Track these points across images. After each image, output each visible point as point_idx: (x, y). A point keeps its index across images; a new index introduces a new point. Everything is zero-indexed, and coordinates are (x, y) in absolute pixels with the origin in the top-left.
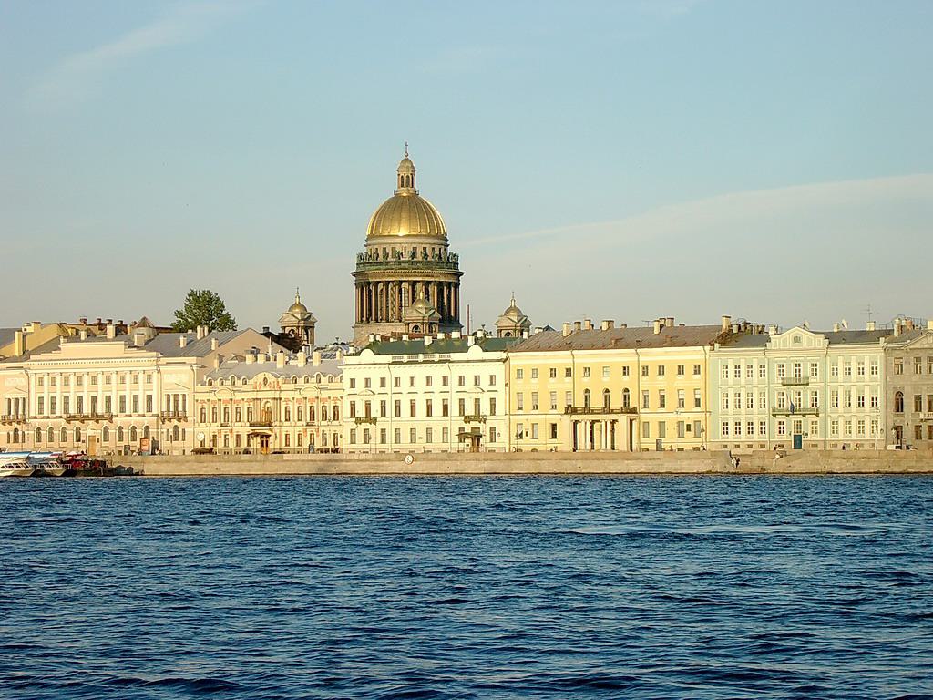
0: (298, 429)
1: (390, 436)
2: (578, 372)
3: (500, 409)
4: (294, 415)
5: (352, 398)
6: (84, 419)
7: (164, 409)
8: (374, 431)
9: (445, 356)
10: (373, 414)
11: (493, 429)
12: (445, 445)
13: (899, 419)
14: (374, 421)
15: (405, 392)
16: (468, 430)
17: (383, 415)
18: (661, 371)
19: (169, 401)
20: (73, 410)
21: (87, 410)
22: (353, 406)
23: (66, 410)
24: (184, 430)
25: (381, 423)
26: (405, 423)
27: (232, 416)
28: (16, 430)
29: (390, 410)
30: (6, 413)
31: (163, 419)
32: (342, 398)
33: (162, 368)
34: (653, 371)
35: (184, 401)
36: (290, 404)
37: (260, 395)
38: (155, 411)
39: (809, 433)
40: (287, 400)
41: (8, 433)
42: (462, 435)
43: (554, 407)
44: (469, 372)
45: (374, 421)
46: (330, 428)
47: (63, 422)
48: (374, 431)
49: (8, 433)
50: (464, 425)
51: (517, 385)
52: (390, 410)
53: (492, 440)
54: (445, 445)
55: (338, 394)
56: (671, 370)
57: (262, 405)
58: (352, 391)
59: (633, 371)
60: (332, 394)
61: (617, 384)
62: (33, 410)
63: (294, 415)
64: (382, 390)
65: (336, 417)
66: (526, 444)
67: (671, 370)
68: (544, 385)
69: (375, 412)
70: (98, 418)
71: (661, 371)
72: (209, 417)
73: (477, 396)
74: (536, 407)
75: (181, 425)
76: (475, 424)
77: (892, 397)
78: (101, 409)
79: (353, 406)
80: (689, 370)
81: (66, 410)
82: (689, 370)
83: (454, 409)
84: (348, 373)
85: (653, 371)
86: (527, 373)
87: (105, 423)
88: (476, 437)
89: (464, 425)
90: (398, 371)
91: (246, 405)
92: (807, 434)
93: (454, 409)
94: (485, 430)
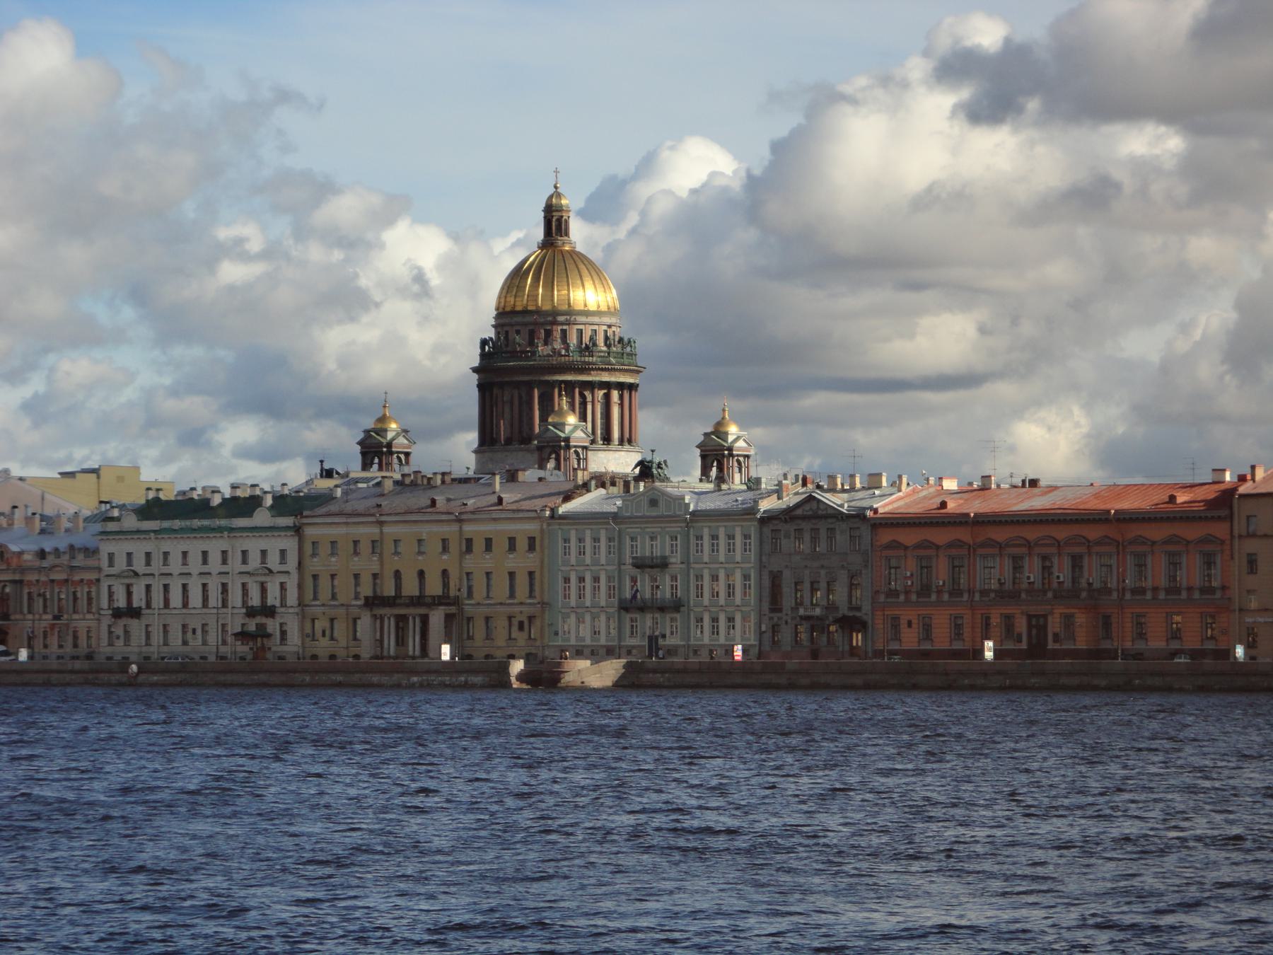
0: (44, 624)
2: (389, 547)
8: (135, 626)
13: (776, 615)
15: (195, 571)
18: (489, 543)
29: (158, 599)
32: (98, 580)
34: (479, 545)
39: (668, 634)
44: (254, 545)
51: (314, 565)
52: (158, 599)
55: (93, 576)
56: (501, 545)
59: (454, 547)
61: (434, 564)
66: (323, 646)
67: (501, 545)
71: (489, 543)
73: (263, 579)
74: (334, 597)
77: (767, 582)
80: (522, 544)
82: (522, 544)
83: (235, 598)
85: (479, 545)
86: (324, 549)
89: (247, 620)
92: (664, 636)
93: (235, 598)
94: (272, 625)
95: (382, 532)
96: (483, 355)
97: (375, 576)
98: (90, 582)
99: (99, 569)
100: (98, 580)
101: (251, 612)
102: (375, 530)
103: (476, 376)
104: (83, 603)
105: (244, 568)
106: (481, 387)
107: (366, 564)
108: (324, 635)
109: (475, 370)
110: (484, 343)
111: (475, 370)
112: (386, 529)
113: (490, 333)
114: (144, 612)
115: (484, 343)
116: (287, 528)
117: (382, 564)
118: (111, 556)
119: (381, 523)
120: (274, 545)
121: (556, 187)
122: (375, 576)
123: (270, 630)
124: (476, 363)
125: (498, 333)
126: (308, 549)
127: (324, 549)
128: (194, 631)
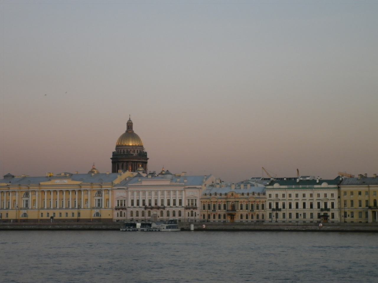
1: (287, 216)
3: (336, 206)
4: (244, 207)
5: (270, 201)
6: (152, 208)
7: (187, 204)
9: (310, 186)
10: (279, 207)
11: (333, 214)
12: (312, 220)
14: (280, 210)
16: (322, 214)
17: (284, 207)
19: (118, 202)
20: (147, 204)
21: (153, 204)
22: (319, 204)
23: (144, 204)
24: (195, 213)
25: (283, 211)
26: (287, 211)
27: (217, 207)
28: (121, 212)
29: (287, 206)
30: (117, 205)
31: (186, 208)
32: (265, 201)
33: (186, 190)
35: (125, 202)
36: (243, 203)
37: (229, 200)
38: (183, 205)
40: (241, 202)
41: (118, 213)
42: (319, 216)
43: (360, 206)
44: (322, 193)
45: (280, 210)
46: (260, 212)
47: (143, 209)
48: (280, 214)
49: (118, 213)
50: (320, 212)
51: (343, 198)
52: (287, 206)
53: (333, 217)
54: (312, 220)
55: (264, 200)
57: (231, 204)
58: (270, 199)
60: (261, 200)
62: (130, 204)
63: (244, 207)
64: (284, 199)
65: (263, 208)
68: (356, 198)
69: (280, 206)
70: (158, 208)
72: (207, 207)
75: (194, 211)
76: (326, 212)
78: (159, 204)
79: (319, 204)
81: (150, 204)
83: (315, 206)
84: (268, 193)
87: (162, 210)
88: (326, 216)
90: (290, 192)
91: (223, 204)
93: (315, 206)
94: (329, 214)
95: (369, 189)
96: (113, 155)
97: (367, 201)
98: (263, 202)
99: (266, 198)
100: (265, 201)
101: (322, 210)
102: (367, 189)
103: (111, 160)
104: (260, 207)
105: (319, 198)
106: (113, 162)
107: (364, 198)
108: (349, 216)
109: (111, 159)
110: (113, 153)
111: (111, 159)
112: (371, 189)
113: (115, 150)
114: (282, 210)
115: (113, 153)
116: (367, 187)
117: (369, 197)
118: (270, 196)
119: (369, 187)
120: (329, 193)
121: (130, 119)
122: (367, 201)
123: (328, 215)
124: (111, 157)
125: (116, 150)
126: (342, 193)
127: (349, 194)
128: (301, 215)
